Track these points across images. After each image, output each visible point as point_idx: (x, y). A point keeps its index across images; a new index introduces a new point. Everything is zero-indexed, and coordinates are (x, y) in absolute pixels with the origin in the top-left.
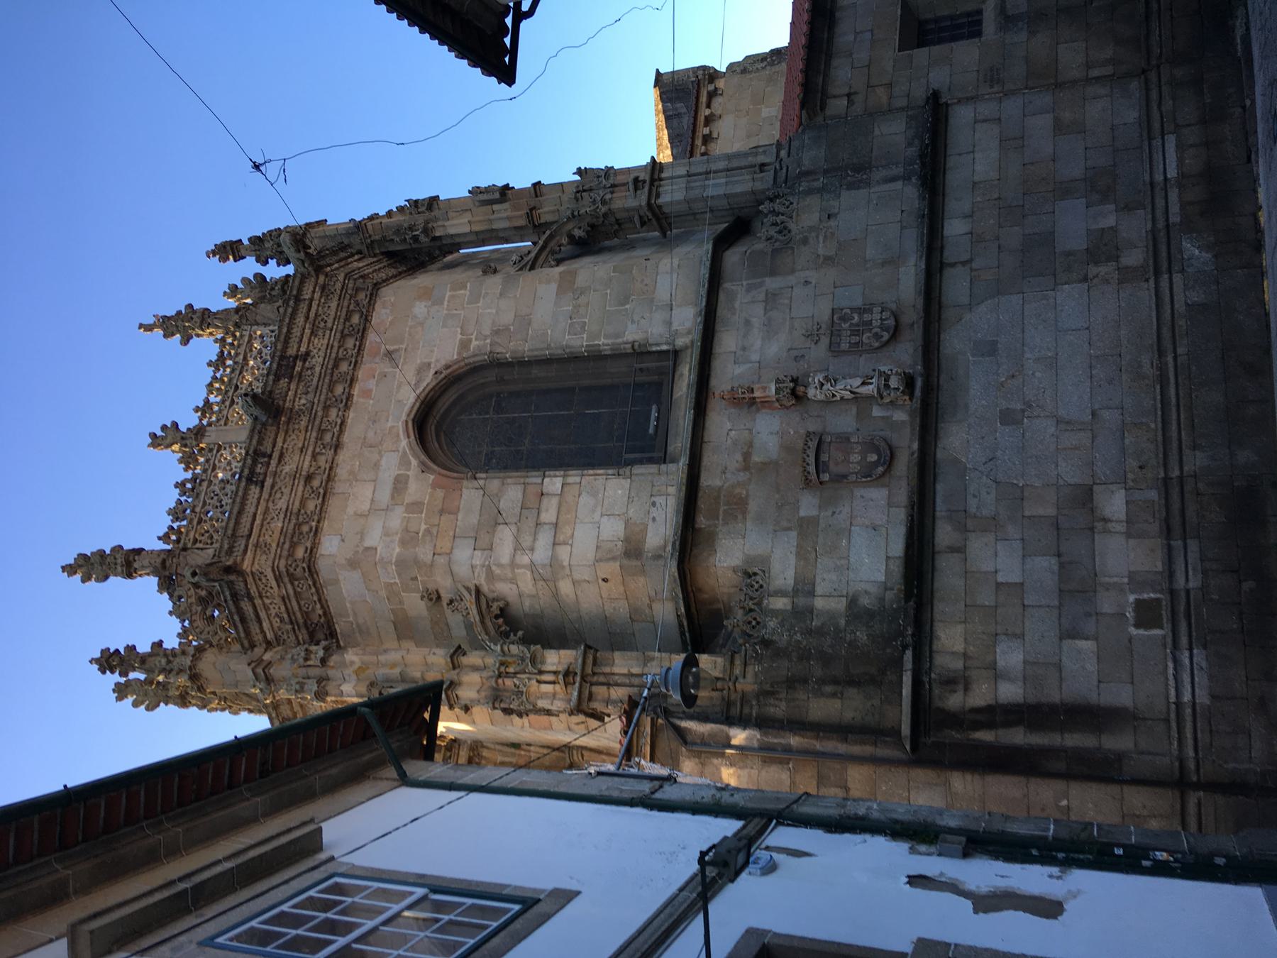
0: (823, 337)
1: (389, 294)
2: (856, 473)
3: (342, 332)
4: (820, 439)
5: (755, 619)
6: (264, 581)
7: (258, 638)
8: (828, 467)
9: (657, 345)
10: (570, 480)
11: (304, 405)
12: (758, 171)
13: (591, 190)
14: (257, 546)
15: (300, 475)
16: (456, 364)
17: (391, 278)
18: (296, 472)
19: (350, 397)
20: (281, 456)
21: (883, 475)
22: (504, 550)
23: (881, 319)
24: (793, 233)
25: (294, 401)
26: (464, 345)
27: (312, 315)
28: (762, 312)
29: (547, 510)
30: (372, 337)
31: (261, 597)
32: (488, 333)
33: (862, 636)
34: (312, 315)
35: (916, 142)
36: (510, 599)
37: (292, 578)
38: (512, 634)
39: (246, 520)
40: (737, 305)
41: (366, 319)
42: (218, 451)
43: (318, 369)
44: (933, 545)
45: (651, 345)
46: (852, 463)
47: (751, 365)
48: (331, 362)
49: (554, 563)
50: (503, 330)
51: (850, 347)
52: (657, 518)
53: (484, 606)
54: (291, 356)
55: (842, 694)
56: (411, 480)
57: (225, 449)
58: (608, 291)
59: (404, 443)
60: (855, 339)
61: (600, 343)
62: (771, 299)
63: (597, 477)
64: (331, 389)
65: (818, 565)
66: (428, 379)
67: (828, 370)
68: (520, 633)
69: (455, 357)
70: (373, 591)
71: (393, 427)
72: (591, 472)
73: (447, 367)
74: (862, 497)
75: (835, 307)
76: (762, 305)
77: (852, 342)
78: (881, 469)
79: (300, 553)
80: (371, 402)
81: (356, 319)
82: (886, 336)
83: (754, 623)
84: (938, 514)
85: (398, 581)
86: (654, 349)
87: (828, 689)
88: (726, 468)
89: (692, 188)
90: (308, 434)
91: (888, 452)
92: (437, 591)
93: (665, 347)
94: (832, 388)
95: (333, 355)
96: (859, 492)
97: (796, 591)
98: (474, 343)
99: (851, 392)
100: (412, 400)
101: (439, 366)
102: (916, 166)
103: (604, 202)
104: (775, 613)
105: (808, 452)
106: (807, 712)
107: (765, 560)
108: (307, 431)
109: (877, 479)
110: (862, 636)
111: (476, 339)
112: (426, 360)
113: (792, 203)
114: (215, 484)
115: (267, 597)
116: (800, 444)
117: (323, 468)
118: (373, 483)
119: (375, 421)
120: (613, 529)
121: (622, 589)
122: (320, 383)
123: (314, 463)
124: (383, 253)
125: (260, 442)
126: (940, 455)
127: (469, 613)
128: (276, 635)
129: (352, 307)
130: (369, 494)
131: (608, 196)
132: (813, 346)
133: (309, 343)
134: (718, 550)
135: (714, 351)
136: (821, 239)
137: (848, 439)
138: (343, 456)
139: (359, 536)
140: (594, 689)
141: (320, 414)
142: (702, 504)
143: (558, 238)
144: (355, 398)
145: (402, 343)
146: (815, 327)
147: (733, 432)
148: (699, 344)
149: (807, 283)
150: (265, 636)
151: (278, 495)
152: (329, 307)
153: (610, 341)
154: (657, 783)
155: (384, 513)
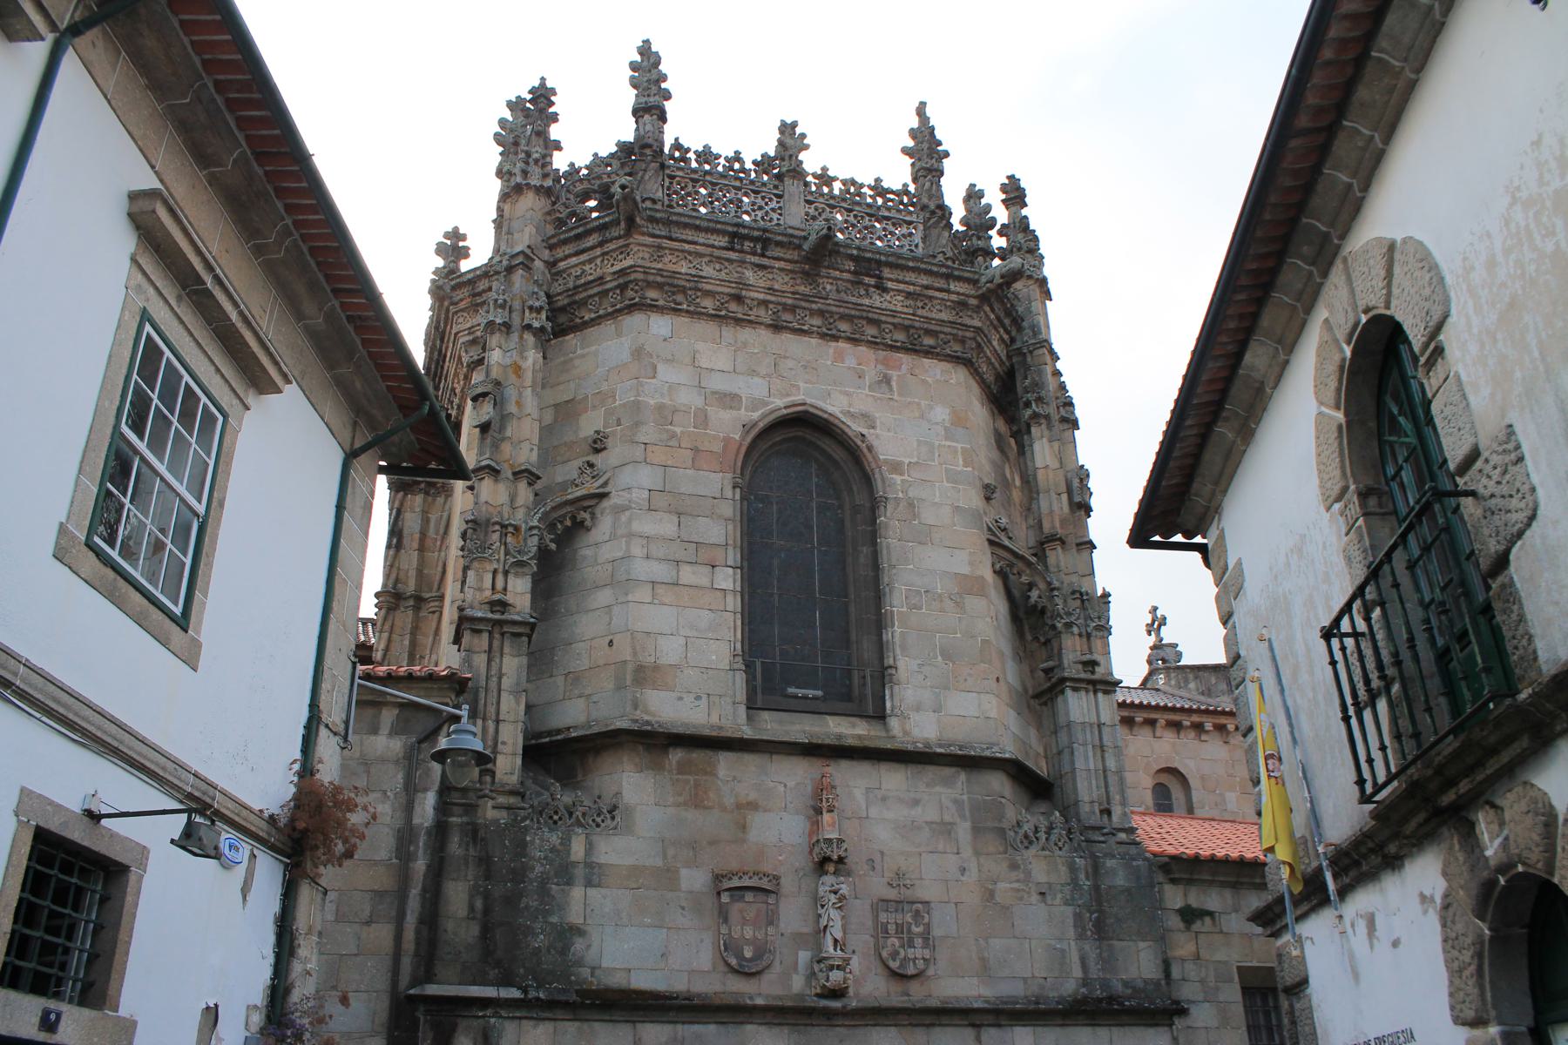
0: (895, 891)
1: (958, 377)
2: (730, 934)
3: (914, 327)
4: (773, 892)
5: (560, 819)
6: (620, 257)
7: (560, 253)
8: (738, 901)
9: (892, 696)
10: (730, 599)
11: (824, 288)
12: (1102, 807)
13: (1084, 608)
14: (660, 247)
15: (742, 289)
16: (874, 458)
17: (981, 378)
18: (745, 284)
19: (835, 338)
20: (762, 267)
21: (728, 964)
22: (647, 525)
23: (916, 958)
24: (1024, 851)
25: (828, 278)
26: (896, 467)
27: (931, 293)
28: (929, 819)
29: (694, 573)
30: (906, 360)
31: (604, 254)
32: (911, 494)
33: (540, 941)
34: (931, 293)
35: (1129, 991)
36: (593, 531)
37: (623, 288)
38: (552, 536)
39: (689, 234)
40: (938, 789)
41: (929, 353)
42: (775, 195)
43: (867, 301)
44: (644, 1022)
45: (891, 688)
46: (742, 929)
47: (864, 807)
48: (876, 317)
49: (631, 583)
50: (913, 511)
51: (882, 923)
52: (680, 702)
53: (586, 503)
54: (881, 272)
55: (473, 919)
56: (734, 413)
57: (778, 202)
58: (959, 635)
59: (779, 402)
60: (892, 928)
61: (896, 628)
62: (945, 829)
63: (732, 630)
64: (843, 317)
65: (620, 892)
66: (855, 427)
67: (856, 898)
68: (553, 546)
69: (881, 457)
71: (799, 389)
72: (739, 623)
73: (870, 448)
74: (702, 941)
75: (932, 905)
76: (936, 818)
77: (889, 926)
78: (733, 962)
79: (652, 294)
80: (829, 363)
81: (929, 341)
82: (894, 965)
83: (556, 817)
84: (679, 1027)
86: (887, 692)
87: (479, 904)
88: (739, 782)
89: (1084, 730)
90: (790, 295)
91: (754, 970)
92: (605, 449)
93: (888, 705)
94: (830, 904)
95: (883, 318)
96: (708, 939)
97: (589, 865)
98: (898, 478)
99: (826, 927)
100: (830, 409)
101: (871, 438)
102: (1099, 992)
103: (1069, 625)
104: (566, 842)
105: (756, 877)
106: (453, 879)
107: (629, 830)
108: (793, 293)
109: (723, 958)
110: (540, 941)
111: (902, 480)
112: (878, 423)
113: (1060, 849)
114: (736, 194)
115: (603, 261)
116: (767, 867)
117: (750, 313)
118: (732, 370)
119: (805, 367)
120: (670, 651)
121: (601, 662)
122: (850, 306)
123: (756, 303)
124: (1012, 366)
125: (779, 244)
126: (749, 1027)
127: (577, 486)
128: (564, 271)
129: (942, 336)
130: (720, 366)
131: (1075, 630)
132: (885, 880)
133: (898, 290)
134: (642, 774)
136: (1016, 885)
137: (770, 923)
138: (764, 335)
139: (670, 357)
140: (485, 636)
141: (814, 306)
142: (698, 755)
143: (1028, 572)
144: (834, 344)
145: (900, 394)
146: (908, 882)
147: (783, 789)
148: (889, 746)
149: (963, 870)
150: (562, 260)
151: (718, 267)
152: (941, 311)
153: (897, 639)
154: (341, 728)
155: (697, 384)
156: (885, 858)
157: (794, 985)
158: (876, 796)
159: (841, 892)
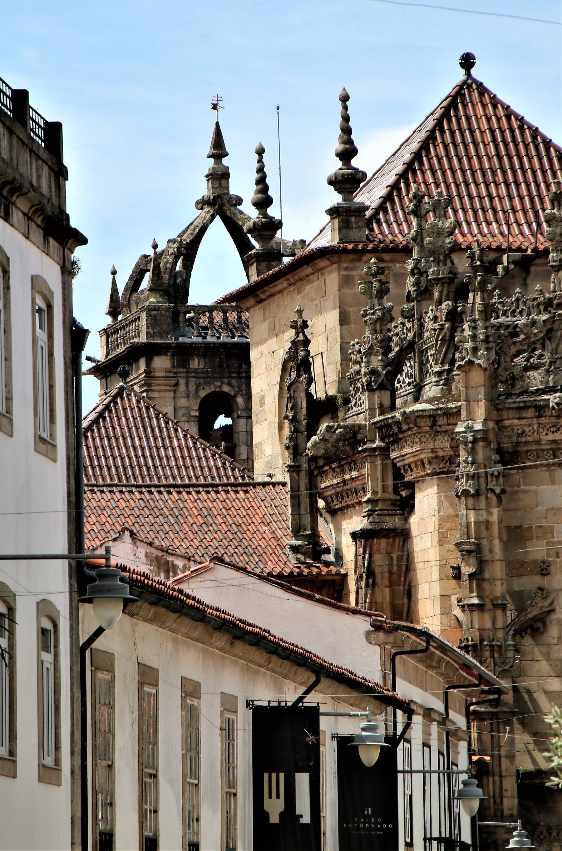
5: (544, 837)
6: (552, 429)
36: (545, 635)
70: (546, 514)
83: (542, 837)
85: (555, 539)
92: (549, 574)
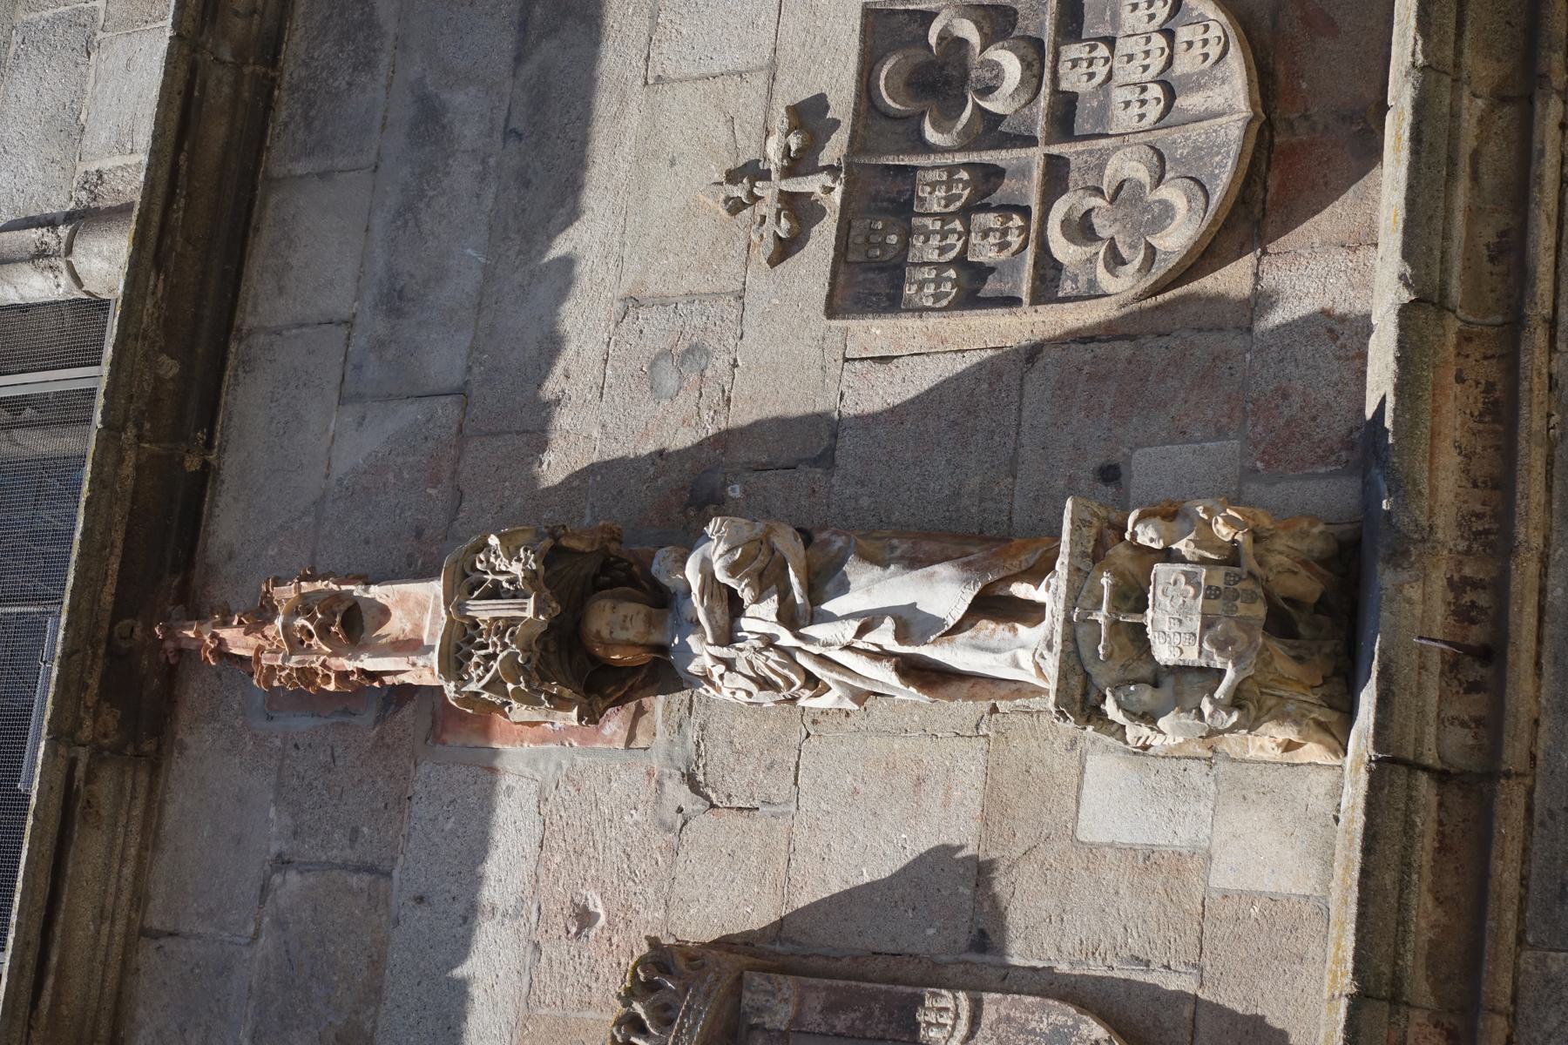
28: (507, 43)
47: (412, 412)
94: (786, 639)
132: (761, 280)
135: (247, 320)
147: (293, 878)
156: (654, 287)
157: (1285, 884)
158: (380, 345)
159: (721, 577)
